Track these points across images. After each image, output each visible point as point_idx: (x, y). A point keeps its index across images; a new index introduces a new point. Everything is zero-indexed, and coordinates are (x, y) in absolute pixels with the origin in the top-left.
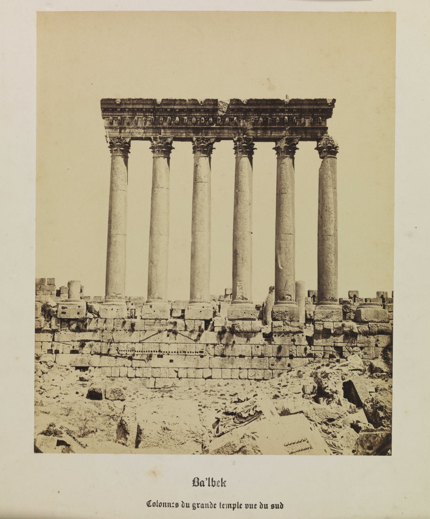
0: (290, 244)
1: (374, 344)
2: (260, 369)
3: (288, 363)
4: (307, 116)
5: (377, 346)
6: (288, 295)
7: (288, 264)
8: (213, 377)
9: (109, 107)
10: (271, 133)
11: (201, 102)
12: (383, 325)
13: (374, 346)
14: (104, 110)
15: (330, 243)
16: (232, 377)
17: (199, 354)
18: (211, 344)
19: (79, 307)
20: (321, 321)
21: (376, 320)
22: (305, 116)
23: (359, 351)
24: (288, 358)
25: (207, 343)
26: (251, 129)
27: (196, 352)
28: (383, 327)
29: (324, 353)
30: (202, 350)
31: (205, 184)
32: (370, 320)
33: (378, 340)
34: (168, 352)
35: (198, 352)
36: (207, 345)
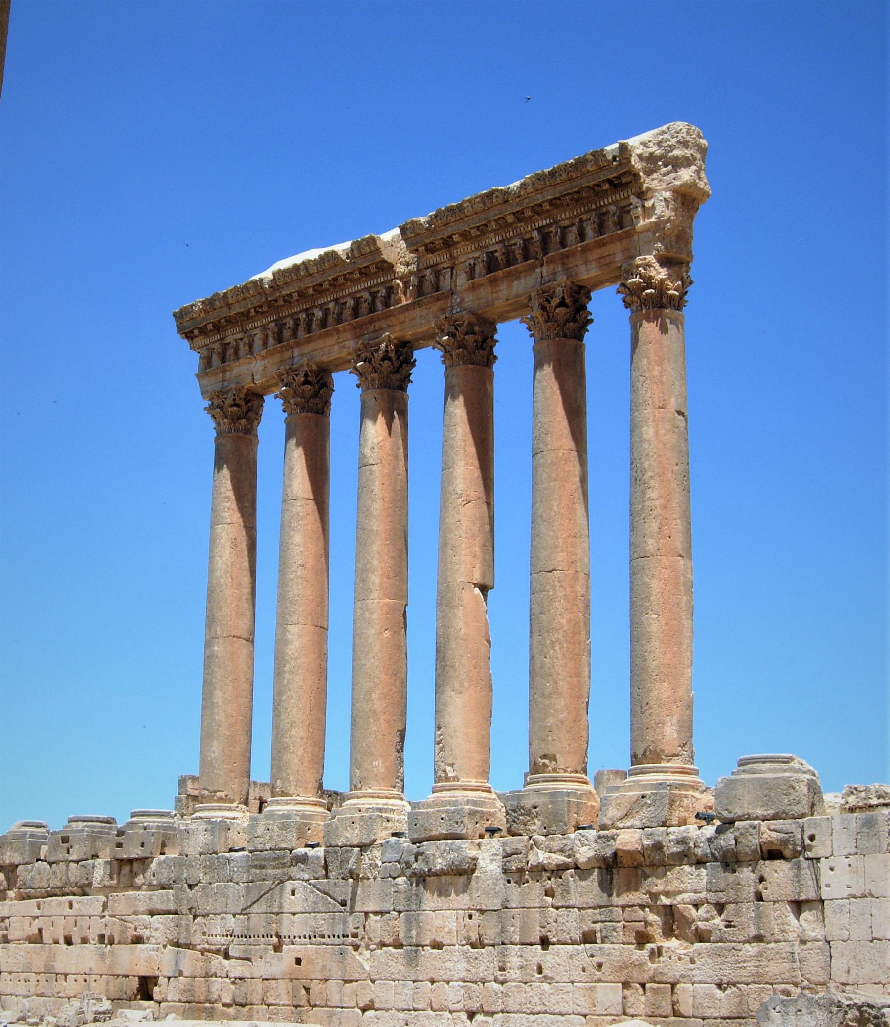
0: (552, 600)
1: (752, 890)
2: (476, 983)
3: (535, 960)
4: (586, 212)
5: (759, 897)
6: (545, 757)
7: (547, 660)
8: (376, 1005)
9: (191, 327)
10: (510, 287)
11: (347, 254)
12: (778, 827)
13: (752, 896)
14: (189, 336)
15: (647, 580)
16: (416, 1006)
17: (350, 939)
18: (376, 913)
19: (145, 828)
20: (613, 826)
21: (760, 812)
22: (583, 214)
23: (713, 917)
24: (539, 947)
25: (366, 909)
26: (466, 290)
27: (344, 936)
28: (774, 834)
29: (624, 926)
30: (355, 931)
31: (374, 468)
32: (740, 813)
33: (762, 879)
34: (292, 937)
35: (347, 937)
36: (367, 914)
